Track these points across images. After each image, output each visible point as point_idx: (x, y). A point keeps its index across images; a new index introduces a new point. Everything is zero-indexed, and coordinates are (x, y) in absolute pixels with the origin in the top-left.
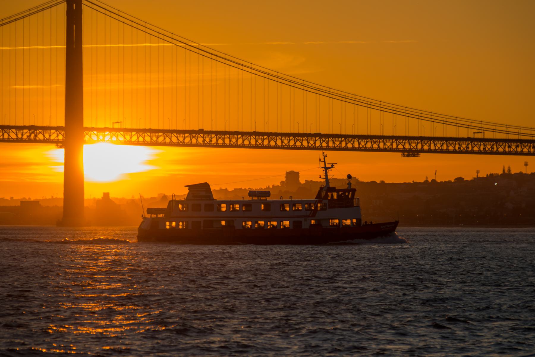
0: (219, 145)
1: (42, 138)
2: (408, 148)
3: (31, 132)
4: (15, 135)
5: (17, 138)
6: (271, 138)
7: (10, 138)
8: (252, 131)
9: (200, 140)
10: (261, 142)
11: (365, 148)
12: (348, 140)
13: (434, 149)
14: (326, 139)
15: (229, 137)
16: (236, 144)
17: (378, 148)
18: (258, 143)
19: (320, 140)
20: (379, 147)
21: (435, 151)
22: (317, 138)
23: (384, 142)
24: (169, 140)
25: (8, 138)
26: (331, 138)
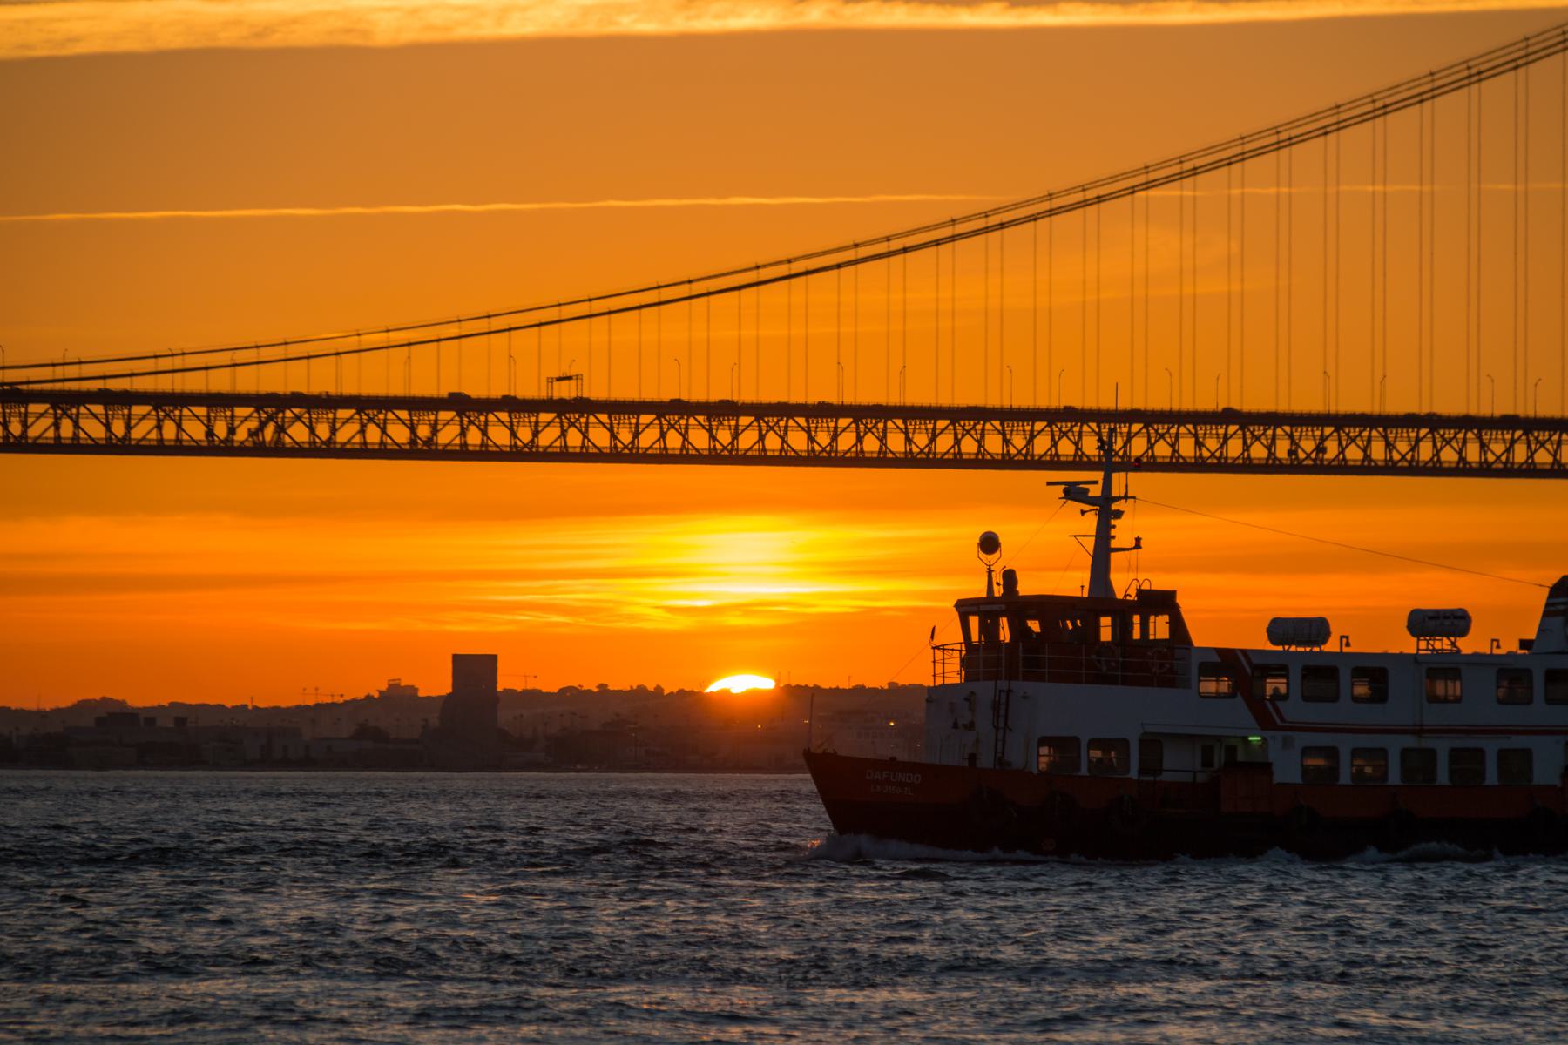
0: (487, 451)
1: (508, 443)
2: (1478, 459)
3: (162, 413)
4: (103, 429)
5: (315, 442)
6: (768, 425)
7: (389, 441)
8: (444, 393)
9: (1090, 447)
10: (1024, 443)
11: (1410, 462)
12: (1348, 435)
13: (1480, 463)
14: (1265, 430)
15: (902, 426)
16: (929, 452)
17: (1363, 461)
18: (1011, 448)
19: (1244, 435)
20: (1367, 457)
21: (1485, 470)
22: (1232, 429)
23: (1385, 437)
24: (878, 443)
25: (178, 440)
26: (1381, 429)
